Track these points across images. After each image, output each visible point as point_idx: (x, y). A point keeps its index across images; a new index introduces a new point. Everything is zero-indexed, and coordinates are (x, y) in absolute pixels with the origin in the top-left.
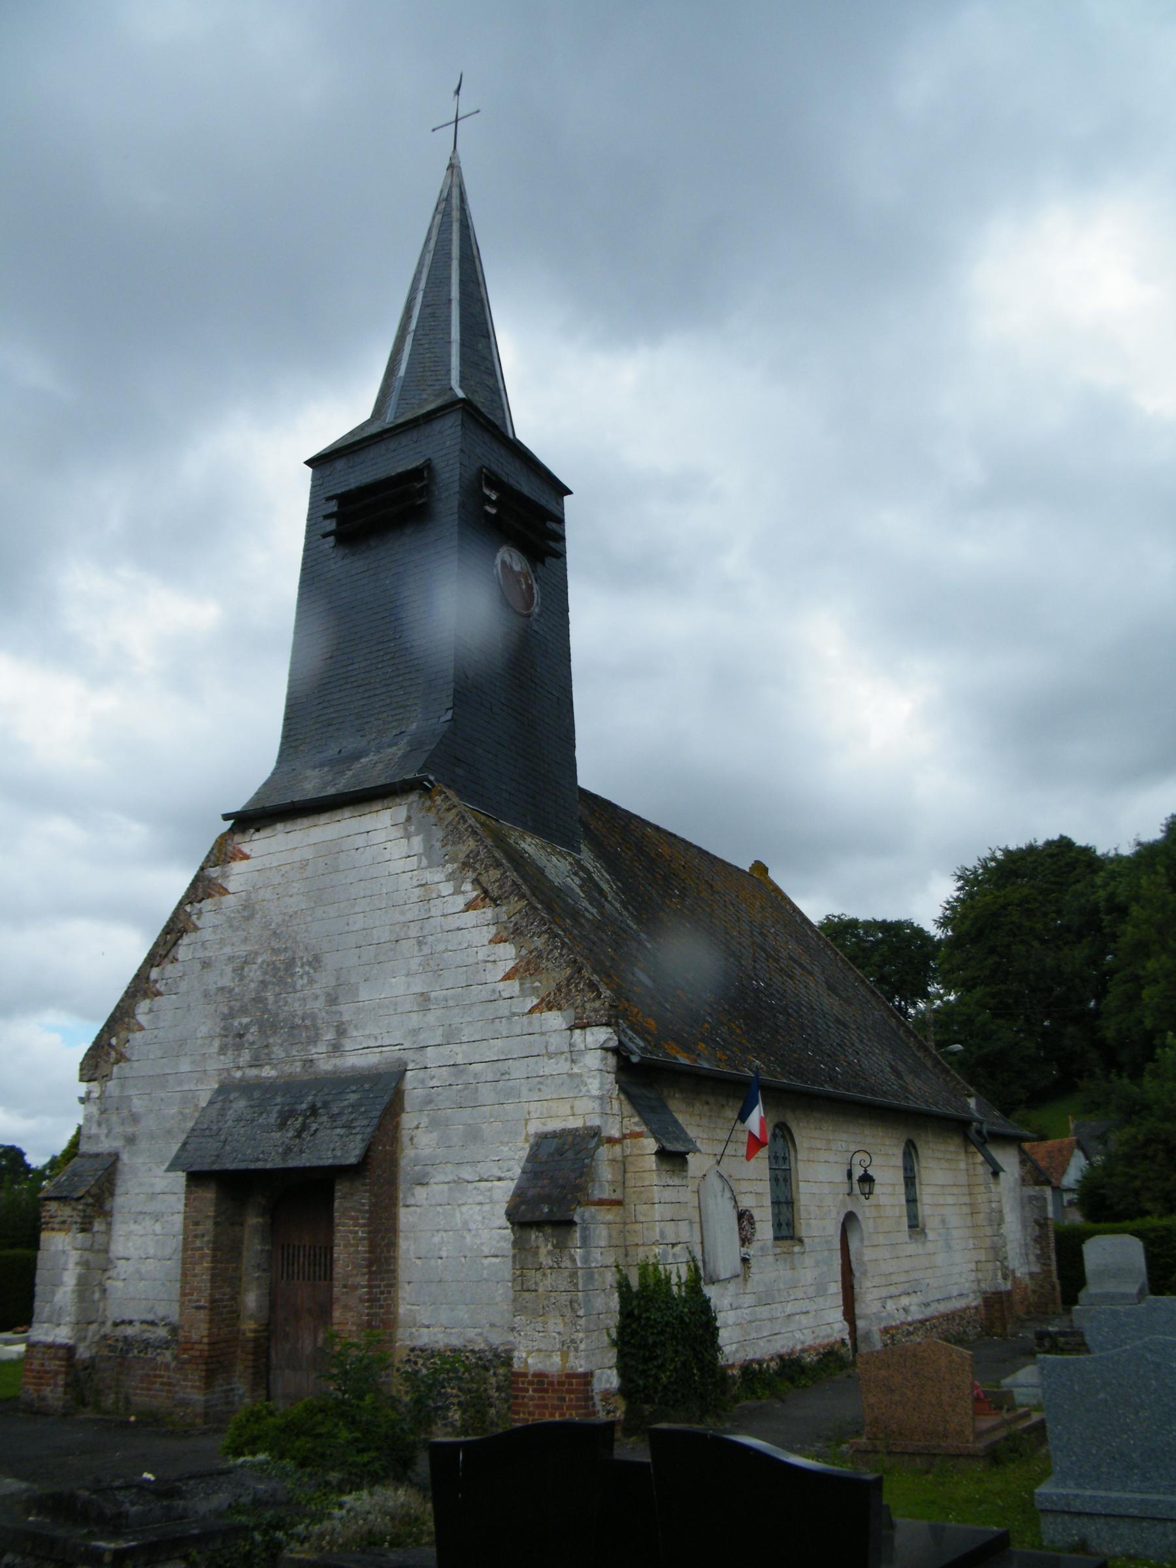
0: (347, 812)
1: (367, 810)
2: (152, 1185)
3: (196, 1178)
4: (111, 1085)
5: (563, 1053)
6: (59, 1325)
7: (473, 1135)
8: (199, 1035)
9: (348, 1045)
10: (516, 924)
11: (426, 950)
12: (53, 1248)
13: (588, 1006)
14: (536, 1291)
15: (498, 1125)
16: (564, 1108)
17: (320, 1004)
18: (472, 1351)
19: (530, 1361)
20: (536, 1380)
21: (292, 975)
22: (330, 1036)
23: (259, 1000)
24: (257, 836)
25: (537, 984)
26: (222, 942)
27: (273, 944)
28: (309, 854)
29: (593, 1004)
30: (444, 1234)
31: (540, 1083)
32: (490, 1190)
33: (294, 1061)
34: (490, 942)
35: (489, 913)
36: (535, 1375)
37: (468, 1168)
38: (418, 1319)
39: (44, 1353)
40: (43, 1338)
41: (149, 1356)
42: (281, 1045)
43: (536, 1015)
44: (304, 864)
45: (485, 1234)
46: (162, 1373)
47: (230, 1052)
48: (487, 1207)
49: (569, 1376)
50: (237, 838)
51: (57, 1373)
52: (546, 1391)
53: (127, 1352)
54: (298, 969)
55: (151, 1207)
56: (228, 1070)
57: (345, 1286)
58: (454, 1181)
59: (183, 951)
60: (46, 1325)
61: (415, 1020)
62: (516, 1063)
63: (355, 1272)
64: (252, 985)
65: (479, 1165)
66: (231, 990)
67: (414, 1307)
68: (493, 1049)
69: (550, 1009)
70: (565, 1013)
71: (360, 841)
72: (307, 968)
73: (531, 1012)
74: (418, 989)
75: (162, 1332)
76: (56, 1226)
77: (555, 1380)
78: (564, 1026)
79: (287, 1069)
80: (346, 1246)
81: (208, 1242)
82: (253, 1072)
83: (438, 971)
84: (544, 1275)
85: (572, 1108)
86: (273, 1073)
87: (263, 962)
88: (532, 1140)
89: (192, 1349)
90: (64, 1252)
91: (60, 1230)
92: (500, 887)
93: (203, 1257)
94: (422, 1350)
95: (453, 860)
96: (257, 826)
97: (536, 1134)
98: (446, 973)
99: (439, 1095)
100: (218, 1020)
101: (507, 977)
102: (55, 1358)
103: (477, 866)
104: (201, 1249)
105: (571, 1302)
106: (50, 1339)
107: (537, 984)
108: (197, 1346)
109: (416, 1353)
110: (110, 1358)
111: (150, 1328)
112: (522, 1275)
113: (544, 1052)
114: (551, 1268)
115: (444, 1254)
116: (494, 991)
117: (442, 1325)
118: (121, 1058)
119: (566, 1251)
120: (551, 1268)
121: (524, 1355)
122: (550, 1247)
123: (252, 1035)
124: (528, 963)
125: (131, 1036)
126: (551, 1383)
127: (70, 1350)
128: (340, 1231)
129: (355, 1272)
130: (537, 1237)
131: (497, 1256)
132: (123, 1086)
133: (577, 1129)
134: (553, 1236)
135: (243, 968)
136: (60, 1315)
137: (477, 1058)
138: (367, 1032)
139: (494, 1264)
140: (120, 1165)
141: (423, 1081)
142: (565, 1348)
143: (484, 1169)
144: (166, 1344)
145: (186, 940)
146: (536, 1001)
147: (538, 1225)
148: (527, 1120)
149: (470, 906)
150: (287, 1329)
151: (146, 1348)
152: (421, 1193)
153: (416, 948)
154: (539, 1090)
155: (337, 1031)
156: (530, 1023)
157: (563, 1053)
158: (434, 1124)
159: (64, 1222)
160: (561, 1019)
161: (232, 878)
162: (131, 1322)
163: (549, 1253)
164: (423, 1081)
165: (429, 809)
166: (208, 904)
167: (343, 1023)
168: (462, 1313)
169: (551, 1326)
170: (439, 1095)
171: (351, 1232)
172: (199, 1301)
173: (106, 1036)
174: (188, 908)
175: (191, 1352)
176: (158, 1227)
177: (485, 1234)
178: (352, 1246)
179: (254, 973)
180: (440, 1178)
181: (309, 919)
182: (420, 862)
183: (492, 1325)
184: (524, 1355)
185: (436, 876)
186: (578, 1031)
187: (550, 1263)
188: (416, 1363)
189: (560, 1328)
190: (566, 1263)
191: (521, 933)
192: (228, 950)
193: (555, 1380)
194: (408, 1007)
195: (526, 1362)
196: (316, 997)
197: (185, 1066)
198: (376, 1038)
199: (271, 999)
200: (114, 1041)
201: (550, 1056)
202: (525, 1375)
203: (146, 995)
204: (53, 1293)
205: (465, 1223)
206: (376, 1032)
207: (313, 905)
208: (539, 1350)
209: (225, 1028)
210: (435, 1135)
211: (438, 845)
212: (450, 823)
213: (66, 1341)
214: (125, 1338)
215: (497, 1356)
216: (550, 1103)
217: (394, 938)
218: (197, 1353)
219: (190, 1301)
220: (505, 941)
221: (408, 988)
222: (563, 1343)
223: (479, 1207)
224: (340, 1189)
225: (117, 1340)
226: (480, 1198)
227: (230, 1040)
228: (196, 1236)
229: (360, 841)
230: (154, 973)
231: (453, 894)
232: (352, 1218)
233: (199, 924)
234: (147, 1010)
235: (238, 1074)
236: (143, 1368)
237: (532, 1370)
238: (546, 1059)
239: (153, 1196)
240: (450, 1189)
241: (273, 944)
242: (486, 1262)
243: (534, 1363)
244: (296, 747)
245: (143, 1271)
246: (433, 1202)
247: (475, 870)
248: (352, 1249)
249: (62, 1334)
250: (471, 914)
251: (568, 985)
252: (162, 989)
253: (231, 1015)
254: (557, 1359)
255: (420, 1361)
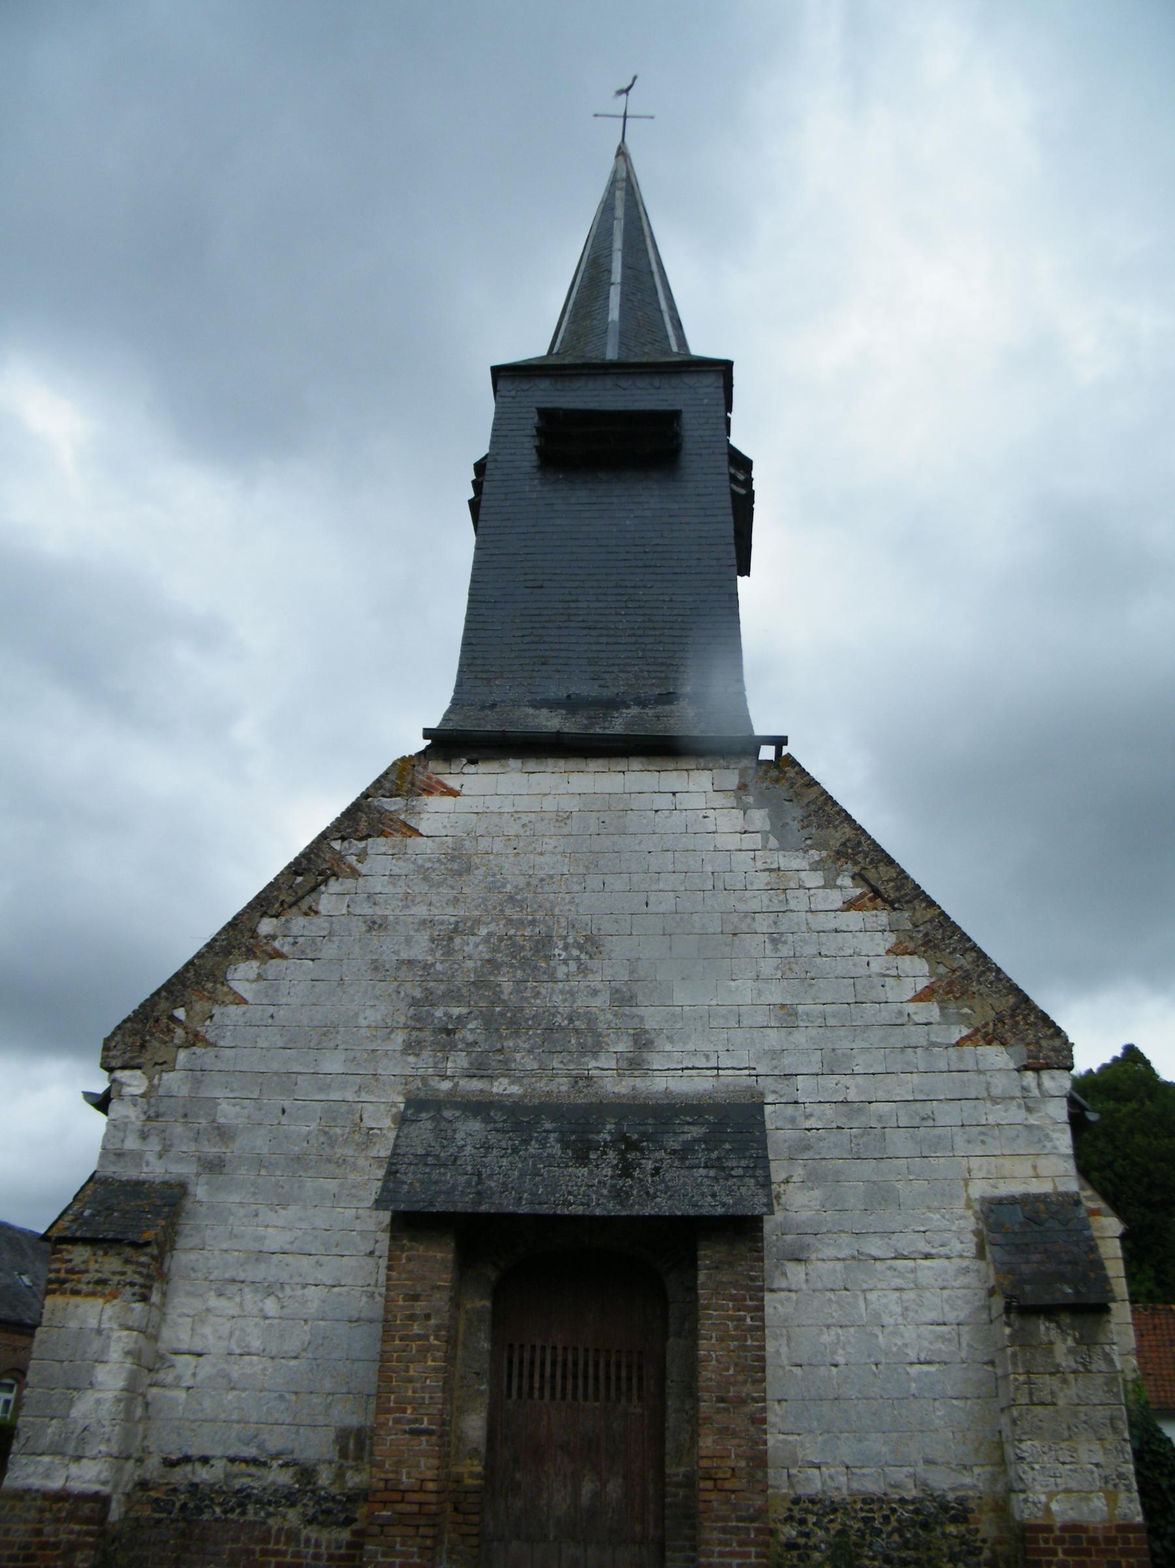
0: (636, 764)
1: (672, 766)
2: (262, 1239)
3: (410, 1224)
4: (172, 1081)
5: (1013, 1098)
6: (78, 1458)
7: (881, 1196)
8: (364, 1023)
9: (656, 1061)
10: (926, 935)
11: (785, 951)
12: (73, 1324)
13: (1044, 1043)
14: (1054, 1404)
15: (921, 1186)
16: (1023, 1168)
17: (601, 1001)
18: (903, 1501)
19: (1054, 1506)
20: (1067, 1535)
21: (548, 958)
22: (623, 1046)
23: (479, 984)
24: (472, 769)
25: (966, 1010)
26: (408, 899)
27: (508, 912)
28: (571, 805)
29: (1051, 1042)
30: (840, 1331)
31: (984, 1134)
32: (913, 1271)
33: (554, 1076)
34: (888, 952)
35: (883, 917)
36: (1065, 1528)
37: (877, 1241)
38: (800, 1456)
39: (41, 1510)
40: (36, 1482)
41: (250, 1516)
42: (530, 1051)
43: (968, 1049)
44: (563, 818)
45: (910, 1333)
46: (282, 1547)
47: (426, 1054)
48: (910, 1295)
49: (1121, 1528)
50: (434, 766)
51: (73, 1547)
53: (200, 1510)
54: (557, 952)
55: (259, 1272)
56: (424, 1079)
57: (721, 1400)
58: (853, 1258)
59: (329, 900)
60: (46, 1459)
61: (774, 1038)
62: (946, 1106)
63: (740, 1378)
64: (470, 964)
65: (894, 1237)
66: (427, 967)
67: (790, 1438)
68: (907, 1086)
69: (989, 1043)
70: (1011, 1050)
71: (664, 802)
72: (575, 952)
73: (958, 1044)
74: (778, 1000)
75: (284, 1478)
76: (83, 1287)
77: (1100, 1535)
78: (1012, 1065)
79: (542, 1085)
80: (721, 1339)
81: (439, 1327)
82: (476, 1085)
83: (809, 980)
84: (1065, 1381)
85: (1035, 1167)
86: (515, 1089)
87: (490, 935)
88: (977, 1207)
89: (402, 1501)
90: (99, 1332)
91: (93, 1294)
92: (898, 889)
93: (425, 1351)
94: (813, 1502)
95: (819, 846)
96: (475, 756)
97: (983, 1200)
98: (822, 983)
99: (821, 1139)
100: (403, 1005)
101: (921, 997)
102: (72, 1517)
103: (859, 858)
104: (425, 1337)
105: (1112, 1419)
106: (56, 1484)
107: (966, 1010)
108: (410, 1497)
109: (802, 1505)
110: (159, 1522)
111: (253, 1470)
112: (1029, 1382)
113: (985, 1095)
114: (1074, 1372)
115: (841, 1360)
116: (900, 1013)
117: (843, 1462)
118: (195, 1039)
119: (1098, 1349)
120: (1074, 1372)
121: (1043, 1498)
122: (1070, 1342)
123: (472, 1031)
124: (951, 983)
125: (216, 1010)
126: (1093, 1541)
127: (102, 1500)
128: (710, 1317)
129: (740, 1378)
130: (1048, 1329)
131: (929, 1363)
132: (197, 1083)
133: (1046, 1195)
134: (1074, 1329)
135: (451, 939)
136: (82, 1441)
137: (881, 1095)
138: (691, 1047)
139: (928, 1374)
140: (188, 1204)
141: (793, 1120)
142: (1110, 1487)
143: (903, 1243)
144: (290, 1498)
145: (334, 886)
146: (966, 1032)
147: (1049, 1311)
148: (966, 1182)
149: (851, 905)
150: (518, 1476)
151: (242, 1505)
152: (796, 1273)
153: (769, 946)
154: (983, 1142)
155: (636, 1042)
156: (961, 1058)
157: (1013, 1098)
158: (814, 1178)
159: (103, 1282)
160: (1006, 1057)
161: (424, 816)
162: (205, 1460)
163: (1071, 1351)
164: (793, 1120)
165: (777, 781)
166: (378, 845)
167: (646, 1032)
168: (877, 1445)
169: (1083, 1455)
170: (821, 1139)
171: (731, 1318)
172: (416, 1421)
173: (163, 1005)
174: (337, 845)
175: (400, 1507)
176: (271, 1306)
177: (910, 1333)
178: (734, 1338)
179: (473, 949)
180: (831, 1252)
181: (576, 888)
182: (766, 840)
183: (928, 1462)
184: (1043, 1498)
185: (793, 861)
186: (1030, 1074)
187: (1074, 1365)
188: (803, 1522)
189: (1099, 1458)
190: (1099, 1365)
191: (936, 947)
192: (421, 911)
193: (1100, 1535)
194: (761, 1020)
195: (1048, 1510)
196: (595, 993)
197: (333, 1064)
198: (707, 1057)
199: (507, 987)
200: (180, 1013)
201: (995, 1100)
202: (1048, 1529)
203: (250, 954)
204: (71, 1403)
205: (876, 1315)
206: (708, 1047)
207: (581, 870)
208: (1068, 1491)
209: (416, 1018)
210: (817, 1193)
211: (796, 825)
212: (813, 802)
213: (96, 1487)
214: (194, 1486)
215: (944, 1507)
216: (1001, 1160)
217: (729, 928)
218: (415, 1508)
219: (397, 1421)
220: (911, 954)
221: (759, 996)
222: (1106, 1480)
223: (897, 1294)
224: (707, 1255)
225: (175, 1490)
226: (899, 1282)
227: (427, 1035)
228: (412, 1317)
229: (664, 802)
230: (266, 926)
231: (823, 887)
232: (732, 1298)
233: (362, 868)
234: (253, 976)
235: (446, 1085)
236: (236, 1540)
237: (1058, 1521)
238: (989, 1104)
239: (261, 1255)
240: (846, 1268)
241: (508, 912)
242: (914, 1370)
243: (1062, 1510)
244: (489, 680)
245: (235, 1375)
246: (819, 1286)
247: (856, 863)
248: (733, 1344)
249: (87, 1475)
250: (853, 914)
251: (1012, 1016)
252: (286, 949)
253: (429, 999)
254: (1099, 1503)
255: (812, 1519)
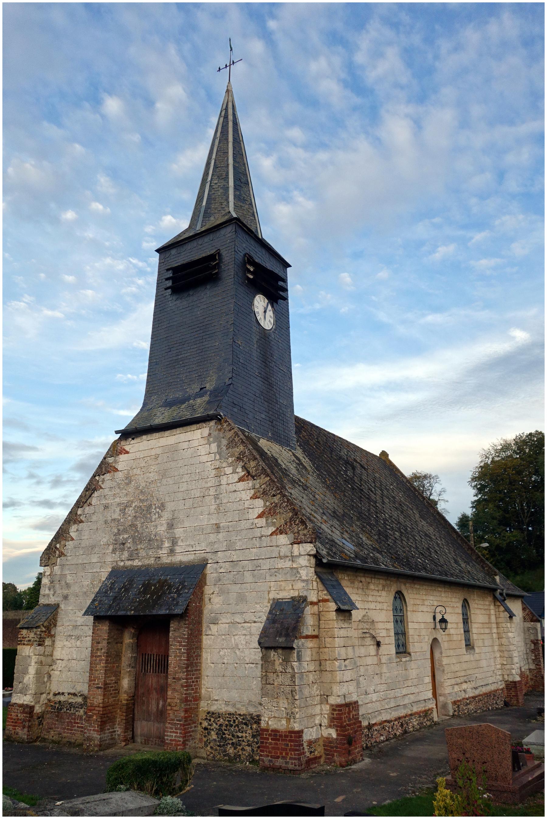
0: (178, 430)
2: (76, 621)
3: (98, 619)
5: (287, 557)
6: (26, 695)
7: (241, 598)
9: (178, 549)
10: (264, 489)
18: (240, 715)
19: (270, 723)
21: (150, 513)
23: (133, 525)
24: (133, 442)
25: (275, 520)
28: (159, 451)
29: (303, 532)
31: (276, 572)
34: (251, 498)
35: (250, 483)
36: (272, 731)
44: (157, 457)
45: (247, 652)
47: (117, 553)
48: (248, 637)
49: (290, 732)
50: (123, 443)
52: (278, 740)
53: (61, 709)
54: (153, 510)
56: (117, 562)
57: (174, 678)
59: (94, 500)
60: (19, 694)
62: (264, 561)
65: (244, 614)
69: (281, 534)
70: (288, 536)
71: (185, 445)
72: (158, 510)
73: (271, 535)
75: (80, 700)
76: (25, 642)
78: (288, 543)
79: (147, 562)
80: (175, 657)
81: (104, 652)
84: (278, 676)
85: (292, 585)
86: (140, 564)
87: (135, 506)
88: (271, 602)
90: (29, 656)
91: (28, 645)
92: (256, 470)
94: (213, 713)
95: (231, 456)
96: (134, 437)
97: (274, 599)
99: (224, 577)
101: (260, 516)
103: (244, 459)
107: (275, 520)
108: (97, 708)
110: (52, 712)
112: (266, 675)
115: (225, 661)
118: (62, 554)
121: (267, 719)
124: (270, 510)
126: (281, 736)
129: (179, 671)
130: (274, 655)
132: (62, 570)
135: (125, 509)
138: (188, 543)
140: (59, 610)
141: (216, 569)
142: (288, 717)
144: (81, 706)
145: (96, 494)
146: (274, 529)
147: (275, 648)
149: (241, 480)
153: (213, 500)
154: (276, 575)
156: (271, 541)
157: (287, 557)
158: (221, 592)
159: (29, 641)
160: (287, 539)
162: (63, 694)
163: (281, 664)
166: (107, 476)
172: (98, 684)
174: (97, 478)
178: (178, 657)
179: (130, 511)
180: (224, 620)
181: (159, 485)
182: (215, 457)
184: (267, 719)
186: (296, 546)
187: (281, 670)
188: (210, 720)
190: (289, 670)
191: (267, 494)
192: (117, 500)
195: (268, 723)
198: (192, 546)
200: (58, 546)
201: (281, 558)
202: (267, 730)
203: (75, 523)
205: (237, 645)
208: (275, 717)
214: (60, 701)
216: (281, 583)
217: (202, 494)
220: (259, 498)
222: (287, 714)
224: (173, 625)
228: (98, 649)
229: (185, 445)
231: (232, 473)
232: (179, 642)
234: (75, 530)
237: (271, 728)
238: (279, 559)
239: (75, 627)
243: (273, 725)
246: (221, 633)
253: (119, 533)
254: (284, 722)
255: (212, 719)
